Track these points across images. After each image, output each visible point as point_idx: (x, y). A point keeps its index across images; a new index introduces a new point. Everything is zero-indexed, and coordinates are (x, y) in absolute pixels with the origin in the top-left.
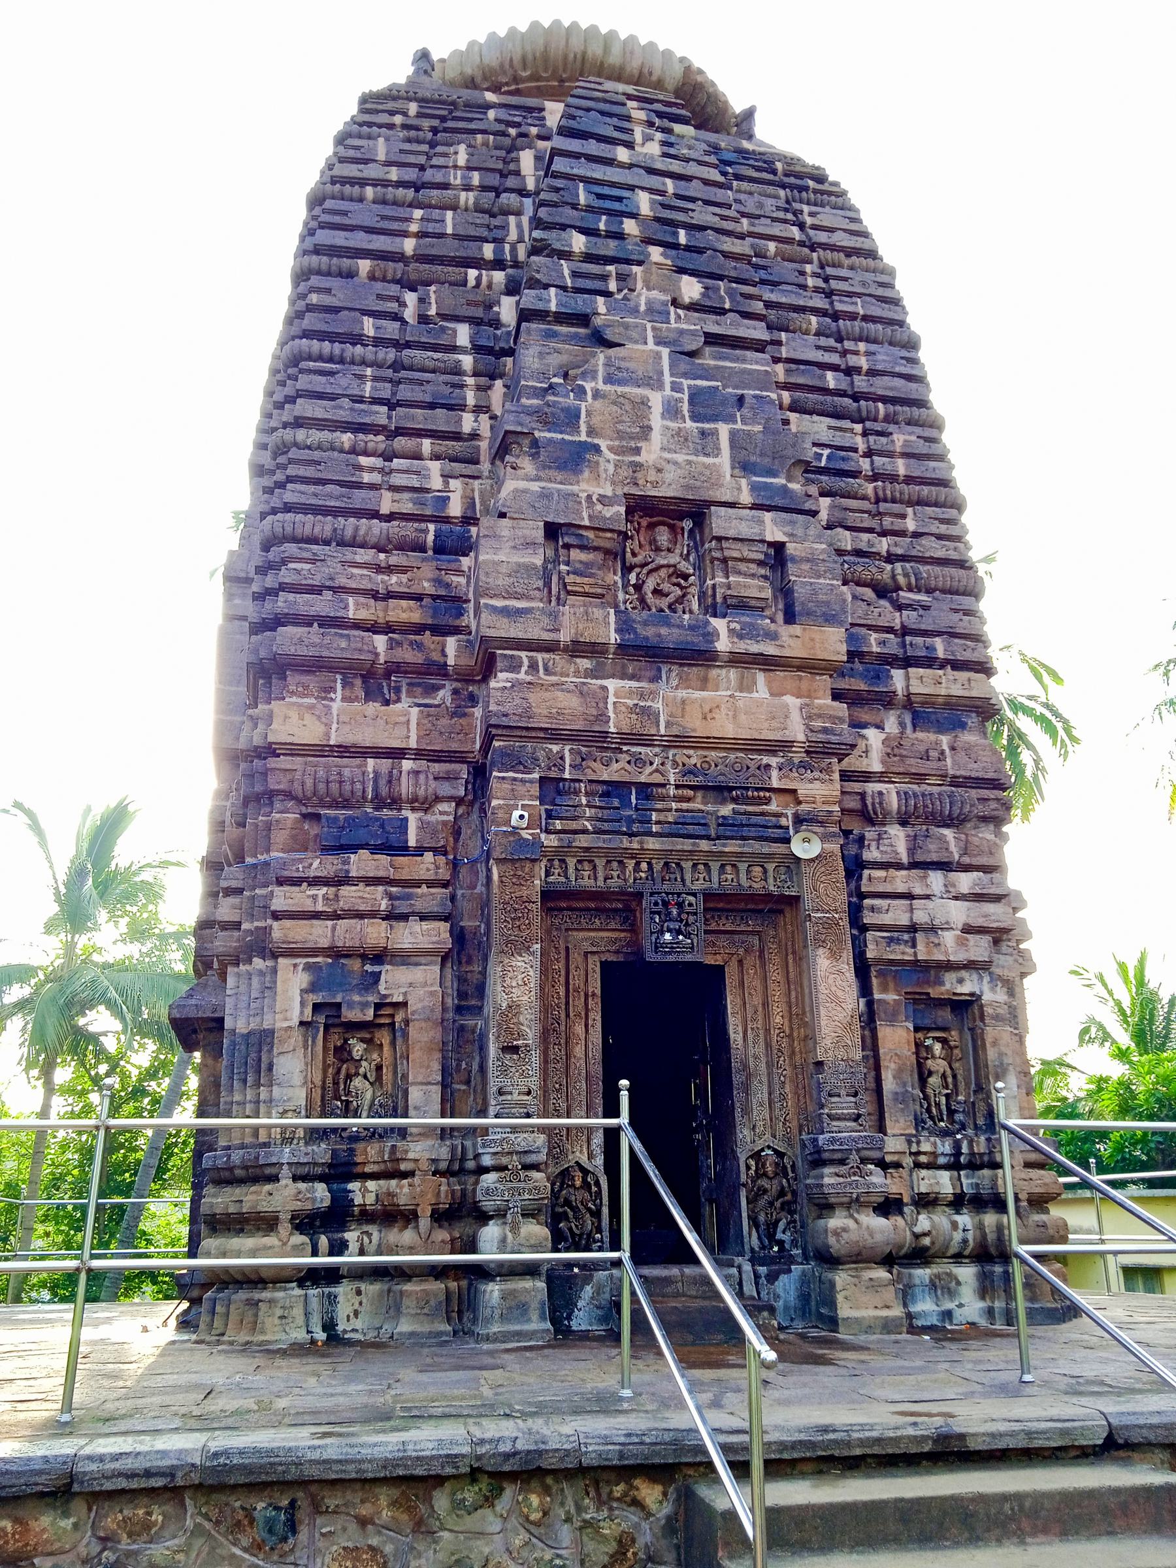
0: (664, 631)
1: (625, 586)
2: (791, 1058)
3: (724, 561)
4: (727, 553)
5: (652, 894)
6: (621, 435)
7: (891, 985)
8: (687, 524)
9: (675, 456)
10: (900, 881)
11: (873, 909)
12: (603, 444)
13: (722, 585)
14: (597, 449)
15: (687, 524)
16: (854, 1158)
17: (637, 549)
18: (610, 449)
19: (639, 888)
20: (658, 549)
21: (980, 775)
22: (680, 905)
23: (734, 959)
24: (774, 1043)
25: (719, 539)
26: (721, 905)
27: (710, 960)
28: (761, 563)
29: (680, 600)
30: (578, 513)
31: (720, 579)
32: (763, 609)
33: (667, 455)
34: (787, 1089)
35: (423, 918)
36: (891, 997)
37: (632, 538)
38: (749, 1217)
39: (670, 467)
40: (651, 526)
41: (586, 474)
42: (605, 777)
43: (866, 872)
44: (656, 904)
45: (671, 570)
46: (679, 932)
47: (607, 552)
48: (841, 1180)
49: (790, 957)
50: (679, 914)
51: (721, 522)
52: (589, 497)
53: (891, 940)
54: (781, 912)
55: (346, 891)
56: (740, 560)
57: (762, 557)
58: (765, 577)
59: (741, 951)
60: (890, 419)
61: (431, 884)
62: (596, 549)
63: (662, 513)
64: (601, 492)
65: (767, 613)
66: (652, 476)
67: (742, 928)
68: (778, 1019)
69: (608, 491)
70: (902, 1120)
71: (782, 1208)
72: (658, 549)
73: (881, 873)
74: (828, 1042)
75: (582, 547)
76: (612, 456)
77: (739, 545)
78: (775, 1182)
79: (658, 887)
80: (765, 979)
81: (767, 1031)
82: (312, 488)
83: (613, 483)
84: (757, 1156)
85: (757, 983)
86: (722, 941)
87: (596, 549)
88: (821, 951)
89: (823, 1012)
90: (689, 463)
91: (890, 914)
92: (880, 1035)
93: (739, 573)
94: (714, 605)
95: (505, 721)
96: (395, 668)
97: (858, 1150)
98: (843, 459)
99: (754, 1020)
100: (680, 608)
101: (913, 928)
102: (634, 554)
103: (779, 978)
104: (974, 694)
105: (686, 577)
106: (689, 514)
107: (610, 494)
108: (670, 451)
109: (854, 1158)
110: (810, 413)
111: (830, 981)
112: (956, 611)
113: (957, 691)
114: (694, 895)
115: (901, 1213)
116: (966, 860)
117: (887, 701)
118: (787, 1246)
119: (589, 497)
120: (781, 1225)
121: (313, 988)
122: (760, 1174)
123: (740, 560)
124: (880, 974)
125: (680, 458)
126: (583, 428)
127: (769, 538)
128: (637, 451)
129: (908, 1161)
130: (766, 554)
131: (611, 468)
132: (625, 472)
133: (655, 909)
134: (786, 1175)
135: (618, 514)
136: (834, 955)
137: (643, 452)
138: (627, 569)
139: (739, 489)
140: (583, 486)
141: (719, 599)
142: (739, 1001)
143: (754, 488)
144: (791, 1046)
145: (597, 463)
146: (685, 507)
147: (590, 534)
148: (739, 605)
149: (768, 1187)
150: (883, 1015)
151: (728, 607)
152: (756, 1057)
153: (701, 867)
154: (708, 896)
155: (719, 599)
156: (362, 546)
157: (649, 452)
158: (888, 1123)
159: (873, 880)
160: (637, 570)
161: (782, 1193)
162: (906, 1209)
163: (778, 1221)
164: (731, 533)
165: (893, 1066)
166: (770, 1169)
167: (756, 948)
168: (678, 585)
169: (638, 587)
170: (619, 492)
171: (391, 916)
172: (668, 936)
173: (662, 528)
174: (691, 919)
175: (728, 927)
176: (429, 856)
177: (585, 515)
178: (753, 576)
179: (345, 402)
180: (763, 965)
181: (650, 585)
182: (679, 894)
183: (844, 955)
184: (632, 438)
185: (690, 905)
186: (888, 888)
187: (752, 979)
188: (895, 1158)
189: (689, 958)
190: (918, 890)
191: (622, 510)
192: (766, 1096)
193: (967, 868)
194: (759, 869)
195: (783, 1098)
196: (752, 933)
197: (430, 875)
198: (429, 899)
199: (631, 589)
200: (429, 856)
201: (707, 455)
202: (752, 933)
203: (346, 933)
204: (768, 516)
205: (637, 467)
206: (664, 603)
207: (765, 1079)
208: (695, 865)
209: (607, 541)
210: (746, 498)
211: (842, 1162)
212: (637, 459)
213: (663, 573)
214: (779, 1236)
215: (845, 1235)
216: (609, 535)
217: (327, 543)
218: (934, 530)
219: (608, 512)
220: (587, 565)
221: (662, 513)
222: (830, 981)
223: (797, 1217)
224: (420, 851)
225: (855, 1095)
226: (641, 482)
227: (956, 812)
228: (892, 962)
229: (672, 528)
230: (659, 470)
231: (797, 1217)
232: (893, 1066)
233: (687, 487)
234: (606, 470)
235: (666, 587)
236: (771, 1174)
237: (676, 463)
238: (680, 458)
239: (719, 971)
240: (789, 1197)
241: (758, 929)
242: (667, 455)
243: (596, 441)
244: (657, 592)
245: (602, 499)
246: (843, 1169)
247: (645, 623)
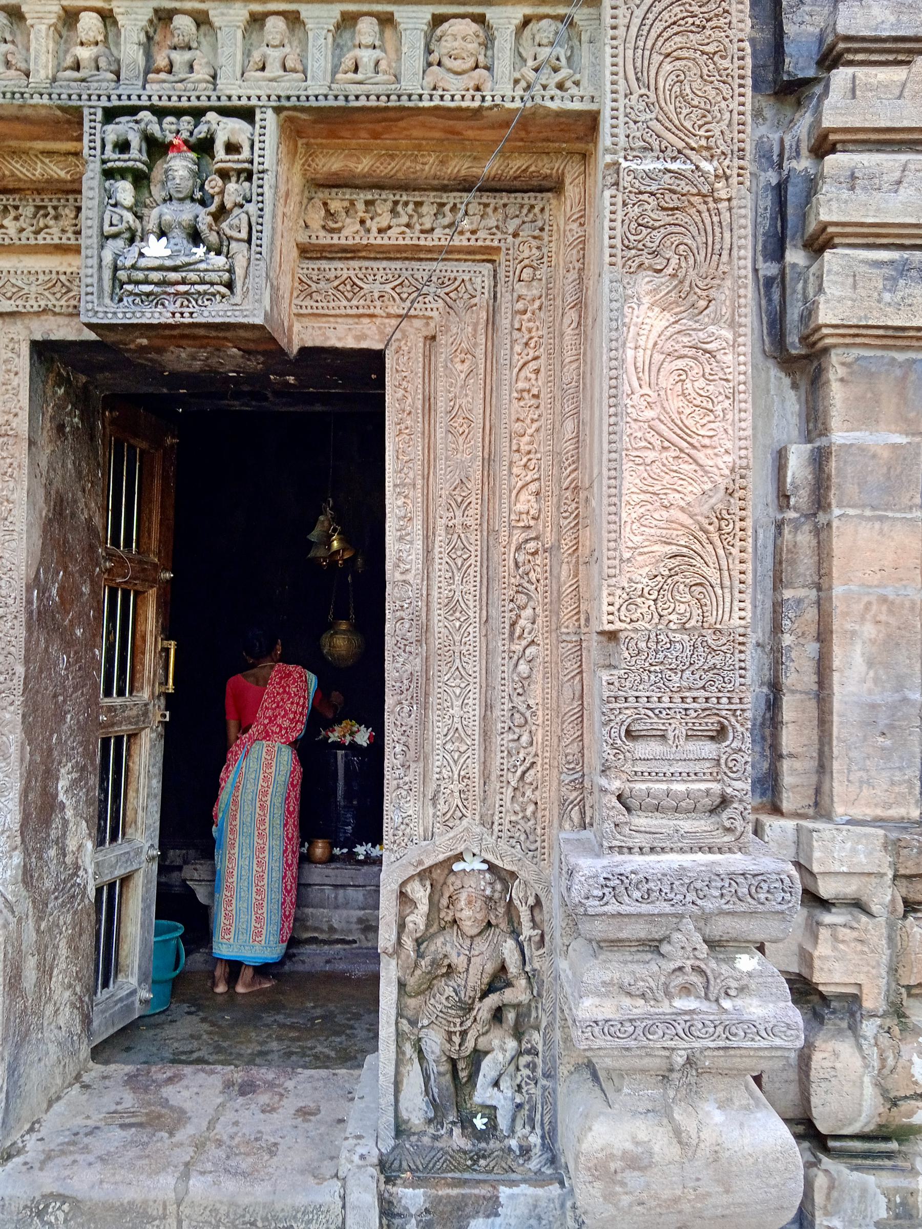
2: (554, 610)
5: (110, 115)
7: (889, 405)
16: (687, 941)
19: (69, 90)
22: (204, 147)
23: (414, 332)
24: (505, 570)
26: (363, 165)
27: (343, 336)
34: (536, 695)
36: (885, 438)
38: (400, 1035)
43: (841, 76)
44: (123, 146)
46: (195, 237)
48: (640, 1007)
49: (573, 315)
50: (199, 175)
53: (903, 269)
54: (554, 187)
59: (435, 308)
67: (439, 238)
68: (526, 501)
70: (882, 781)
71: (498, 1015)
74: (640, 573)
78: (481, 946)
79: (130, 91)
80: (490, 394)
81: (492, 532)
84: (436, 876)
85: (473, 401)
86: (378, 277)
88: (644, 283)
89: (631, 481)
91: (905, 192)
92: (839, 545)
97: (705, 917)
99: (463, 505)
103: (539, 385)
109: (687, 941)
111: (666, 381)
114: (247, 114)
115: (853, 1028)
118: (503, 1123)
120: (488, 1069)
122: (442, 921)
124: (858, 372)
129: (883, 897)
133: (118, 161)
134: (515, 933)
136: (689, 298)
142: (417, 451)
144: (552, 573)
149: (459, 962)
150: (851, 489)
152: (452, 606)
153: (276, 26)
154: (313, 125)
158: (839, 786)
161: (499, 980)
162: (869, 1028)
163: (478, 1056)
165: (869, 630)
166: (469, 915)
167: (482, 300)
172: (156, 249)
174: (234, 190)
175: (393, 238)
180: (491, 354)
182: (198, 114)
183: (723, 295)
185: (232, 148)
187: (458, 385)
188: (850, 889)
189: (214, 312)
192: (475, 711)
194: (468, 27)
195: (520, 719)
196: (469, 253)
202: (469, 253)
207: (474, 667)
208: (257, 20)
214: (483, 1094)
215: (633, 1179)
222: (666, 381)
223: (536, 1038)
225: (720, 734)
228: (896, 336)
231: (536, 1038)
232: (869, 630)
236: (469, 928)
240: (518, 993)
241: (483, 239)
246: (648, 970)
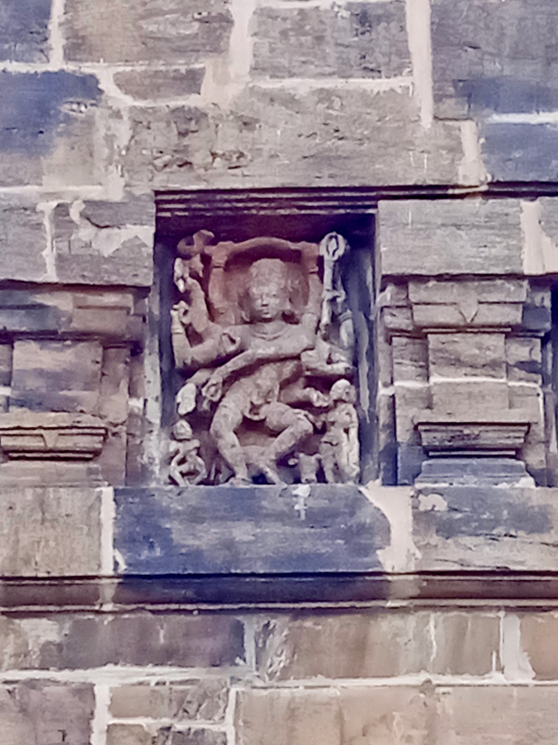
1: (169, 417)
3: (419, 334)
4: (423, 316)
6: (151, 47)
8: (332, 248)
9: (288, 83)
12: (105, 74)
13: (413, 397)
14: (88, 87)
15: (332, 248)
17: (201, 323)
18: (123, 83)
20: (255, 319)
25: (401, 281)
28: (513, 332)
29: (307, 444)
30: (32, 252)
31: (408, 383)
32: (518, 453)
33: (268, 84)
37: (186, 297)
39: (277, 112)
40: (241, 261)
41: (60, 151)
45: (289, 368)
47: (109, 341)
51: (403, 238)
52: (62, 210)
56: (459, 329)
57: (514, 316)
58: (529, 366)
62: (81, 337)
63: (265, 226)
64: (95, 192)
65: (535, 458)
66: (228, 139)
69: (113, 189)
72: (255, 319)
75: (45, 336)
76: (126, 102)
77: (453, 292)
83: (128, 168)
87: (81, 337)
90: (325, 96)
93: (457, 362)
94: (391, 453)
100: (307, 464)
102: (194, 336)
105: (324, 383)
107: (116, 194)
108: (276, 72)
119: (62, 210)
123: (459, 329)
125: (302, 86)
126: (57, 39)
127: (531, 268)
128: (191, 81)
130: (526, 308)
131: (123, 132)
132: (160, 137)
135: (134, 244)
137: (208, 84)
138: (175, 375)
139: (456, 149)
140: (51, 183)
141: (403, 435)
143: (496, 143)
145: (89, 123)
146: (318, 209)
147: (63, 302)
148: (459, 445)
151: (427, 452)
155: (403, 435)
157: (223, 80)
160: (200, 376)
164: (429, 266)
168: (305, 405)
169: (200, 420)
170: (144, 189)
173: (264, 264)
177: (49, 256)
178: (493, 366)
181: (232, 409)
184: (180, 51)
191: (146, 233)
199: (184, 428)
201: (373, 71)
204: (529, 210)
205: (188, 121)
206: (264, 453)
209: (107, 314)
210: (472, 170)
212: (191, 101)
213: (267, 377)
216: (111, 299)
219: (109, 242)
220: (58, 379)
221: (265, 226)
226: (198, 159)
229: (293, 258)
230: (247, 124)
233: (319, 159)
234: (110, 139)
235: (275, 412)
237: (290, 101)
238: (302, 86)
242: (268, 84)
243: (87, 68)
244: (250, 427)
245: (100, 215)
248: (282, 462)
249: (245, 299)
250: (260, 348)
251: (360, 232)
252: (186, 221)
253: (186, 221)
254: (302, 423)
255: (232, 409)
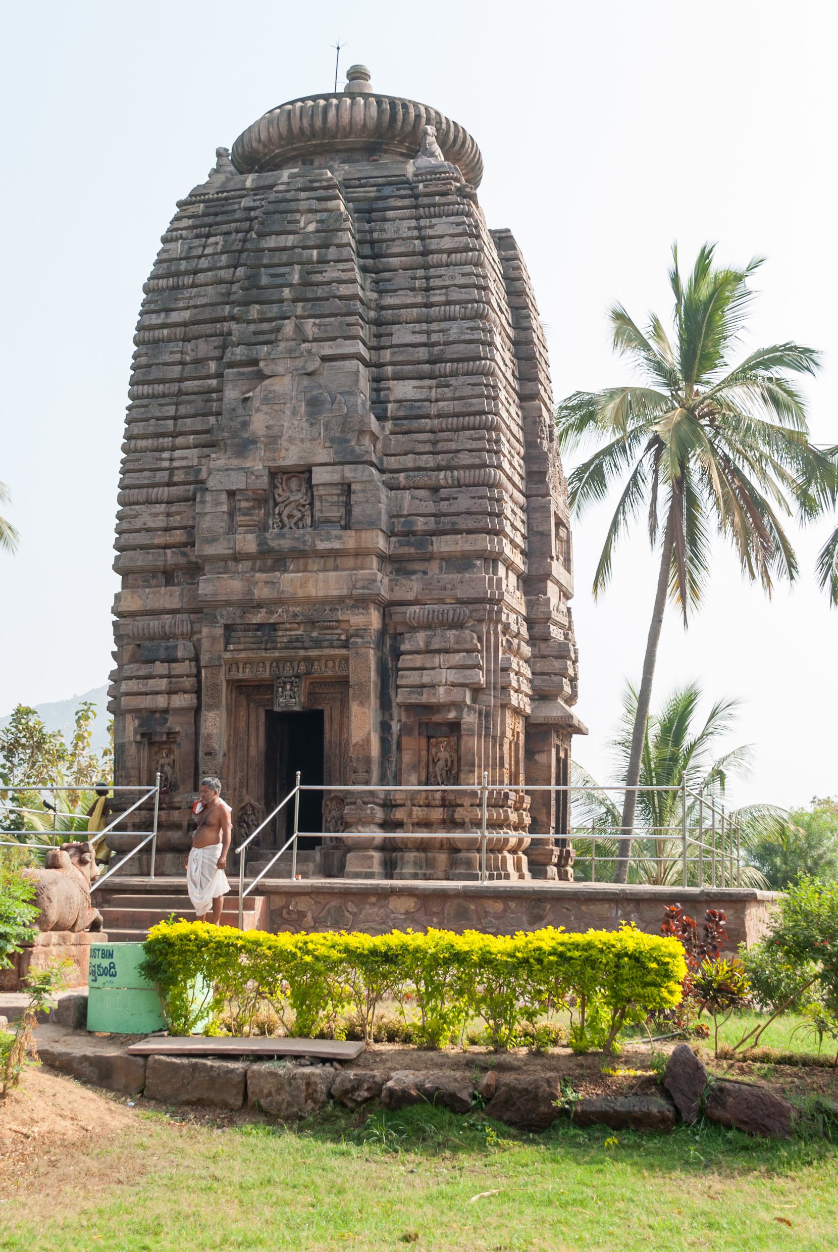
0: (282, 542)
10: (418, 660)
11: (402, 677)
21: (475, 596)
29: (301, 519)
35: (185, 692)
40: (288, 479)
42: (254, 622)
53: (411, 692)
55: (151, 682)
60: (454, 374)
61: (188, 676)
73: (409, 657)
82: (137, 475)
95: (205, 598)
96: (177, 567)
98: (419, 407)
100: (300, 524)
101: (423, 686)
104: (478, 548)
106: (305, 472)
110: (403, 379)
112: (473, 498)
113: (468, 547)
116: (456, 646)
117: (430, 558)
121: (140, 725)
156: (161, 503)
159: (406, 661)
169: (280, 514)
171: (170, 692)
176: (187, 662)
179: (153, 422)
181: (285, 513)
186: (412, 665)
190: (428, 665)
193: (459, 651)
197: (187, 672)
198: (189, 683)
200: (187, 662)
203: (146, 702)
211: (355, 803)
213: (293, 505)
217: (143, 504)
218: (468, 447)
224: (183, 660)
227: (456, 619)
235: (295, 512)
239: (321, 712)
244: (290, 516)
247: (273, 539)
248: (296, 524)
249: (289, 488)
250: (292, 499)
251: (310, 472)
252: (274, 474)
253: (274, 474)
254: (299, 515)
255: (285, 513)
